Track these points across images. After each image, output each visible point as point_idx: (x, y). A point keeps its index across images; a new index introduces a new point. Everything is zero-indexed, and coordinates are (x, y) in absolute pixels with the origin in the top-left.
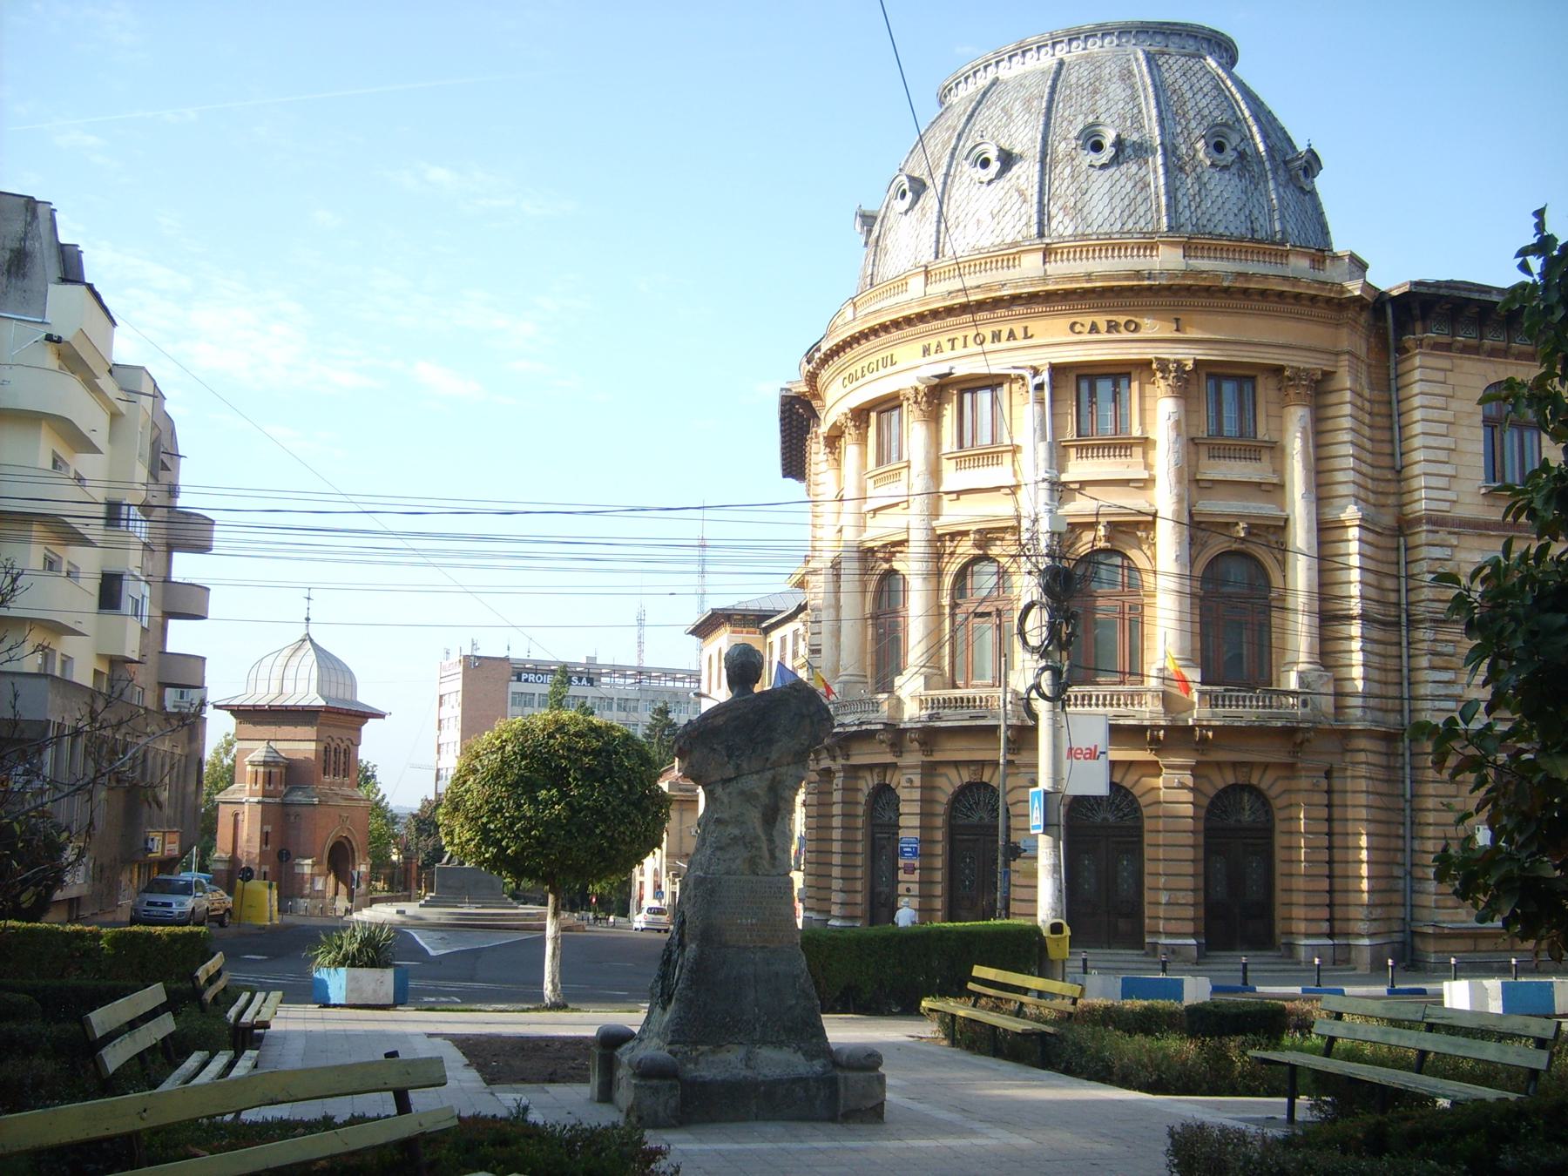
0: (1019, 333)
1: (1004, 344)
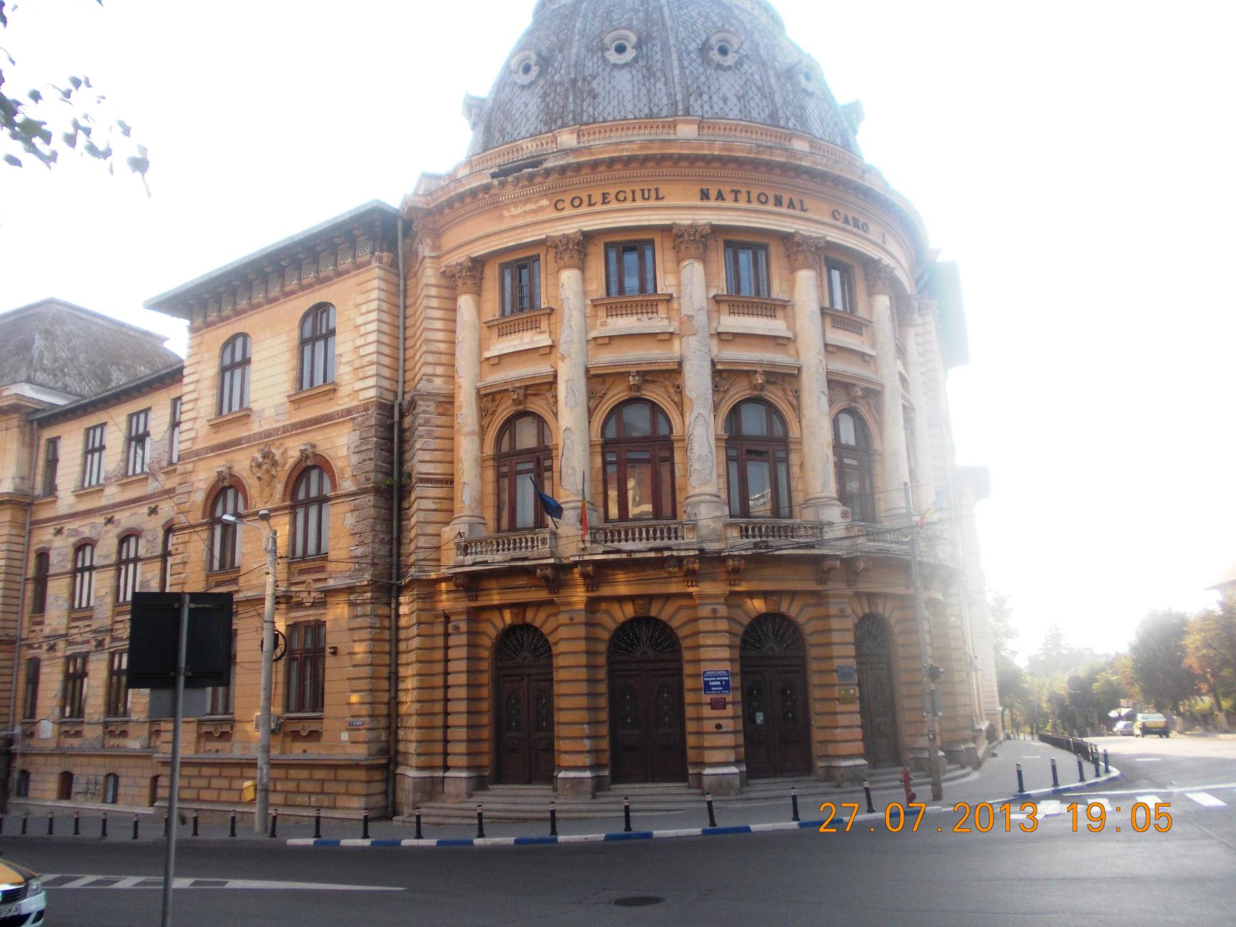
0: (796, 203)
1: (784, 210)
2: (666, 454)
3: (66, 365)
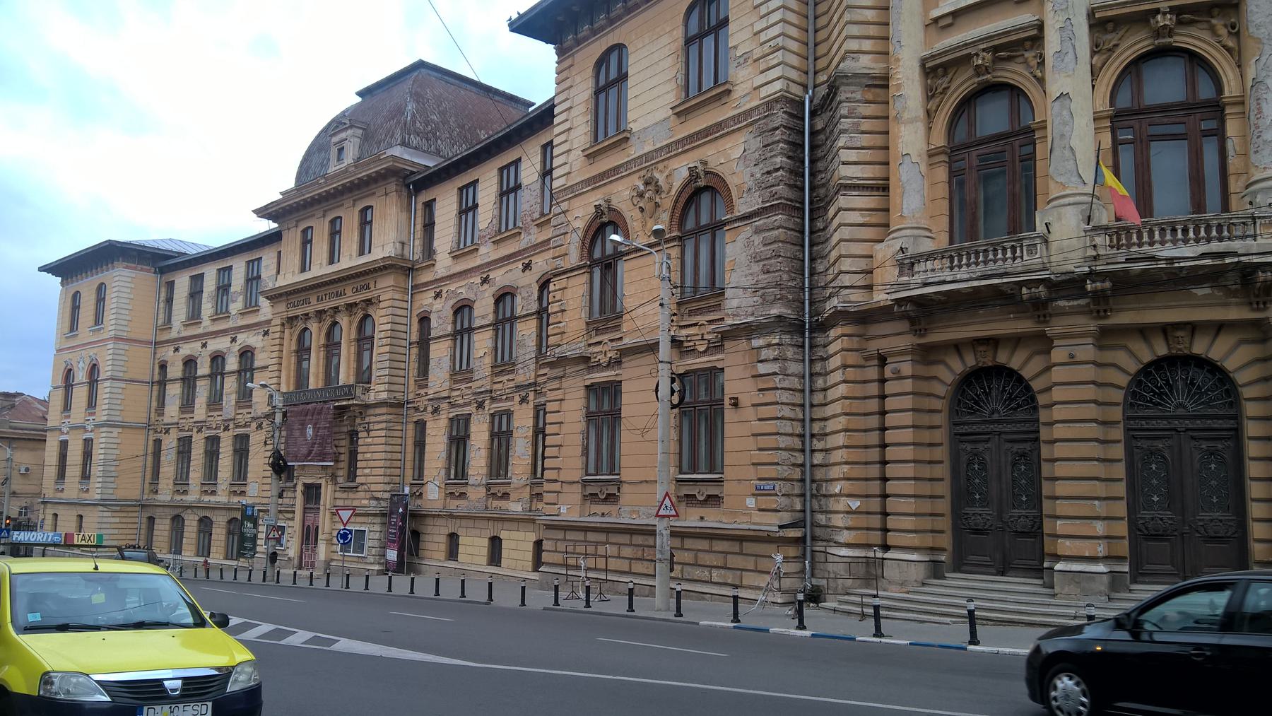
2: (1212, 124)
3: (437, 129)
